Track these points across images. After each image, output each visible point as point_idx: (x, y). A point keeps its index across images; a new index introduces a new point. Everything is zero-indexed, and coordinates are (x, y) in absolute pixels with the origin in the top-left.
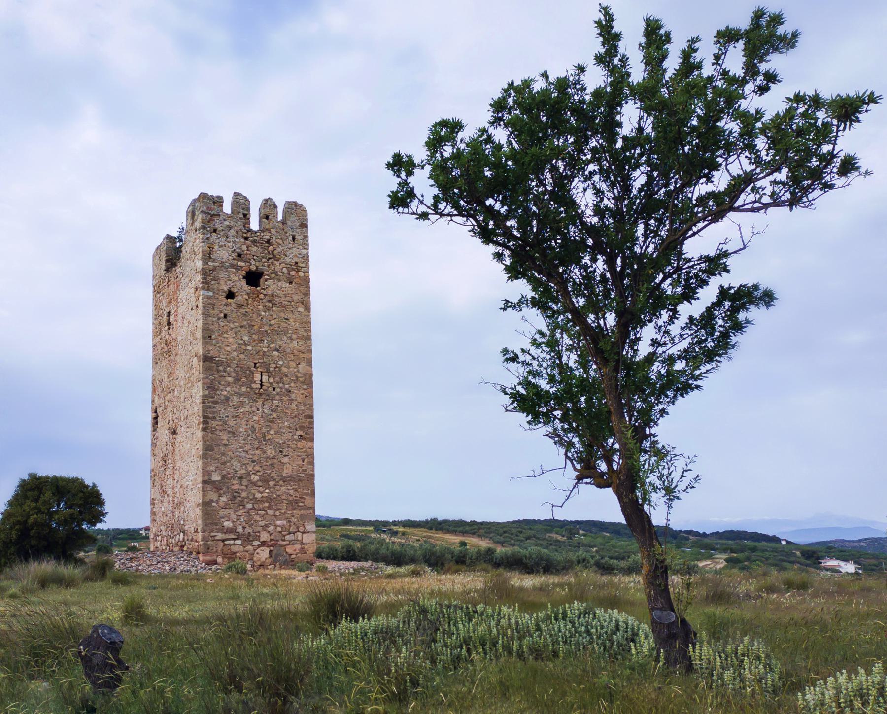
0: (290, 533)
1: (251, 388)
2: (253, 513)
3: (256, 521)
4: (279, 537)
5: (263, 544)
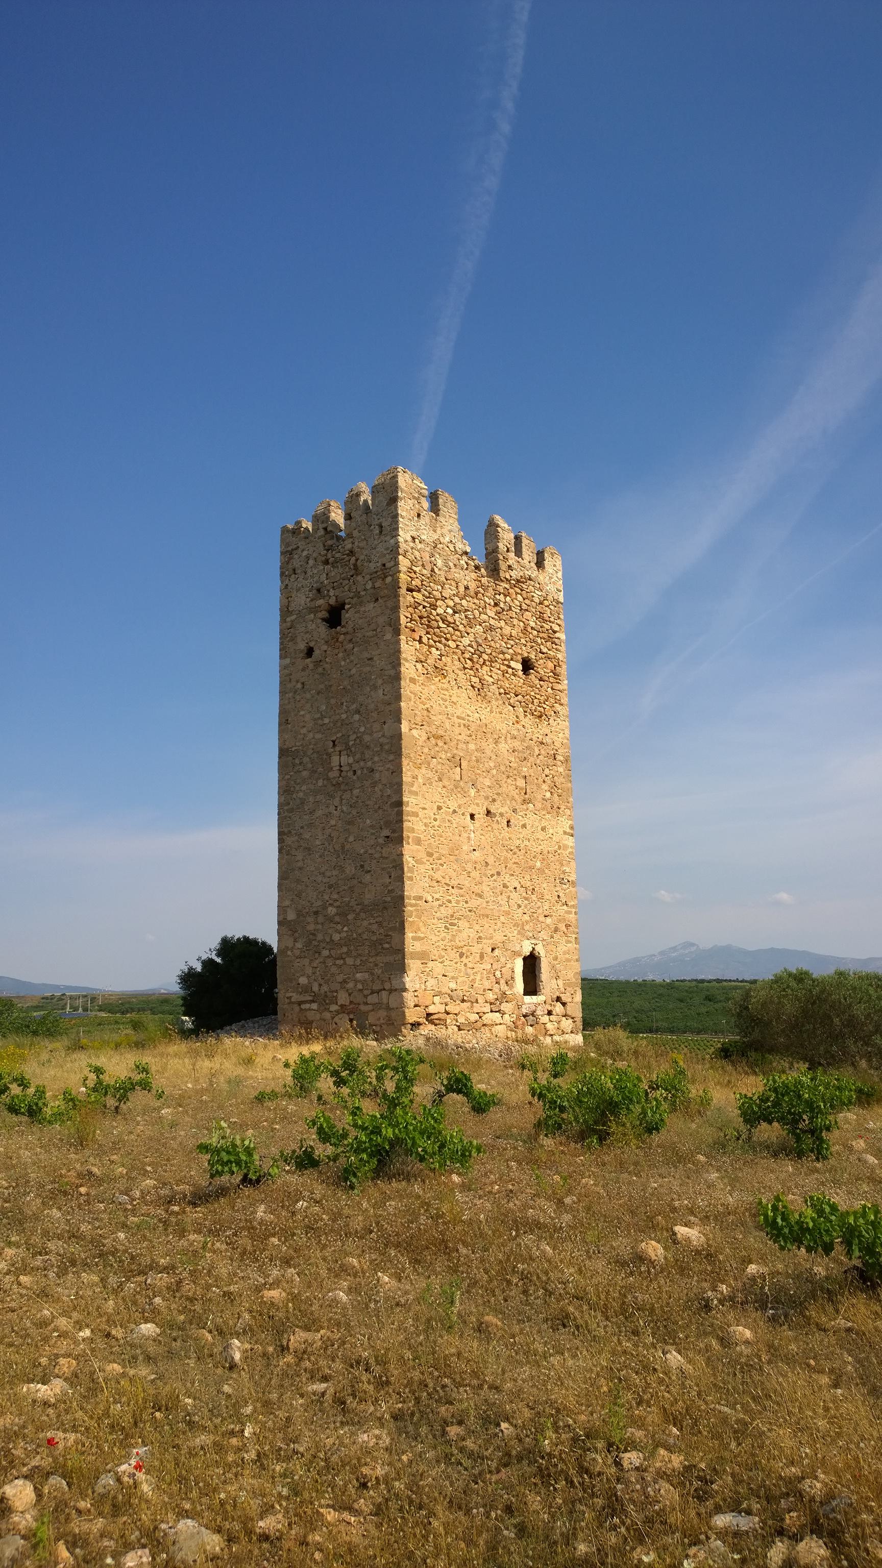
0: (372, 993)
1: (328, 779)
2: (330, 962)
3: (333, 975)
4: (359, 998)
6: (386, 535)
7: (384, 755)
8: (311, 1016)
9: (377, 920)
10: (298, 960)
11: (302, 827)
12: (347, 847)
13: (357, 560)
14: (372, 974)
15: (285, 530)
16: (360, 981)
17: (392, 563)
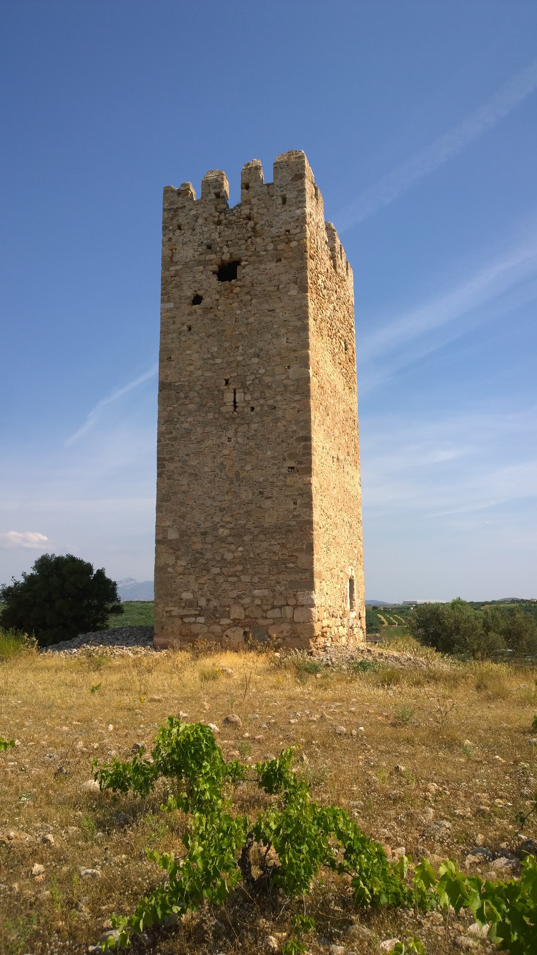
0: (273, 607)
1: (220, 413)
2: (221, 579)
3: (225, 591)
4: (258, 613)
5: (236, 622)
6: (290, 206)
7: (288, 395)
8: (195, 629)
9: (280, 541)
10: (181, 577)
11: (187, 455)
12: (243, 474)
13: (256, 224)
14: (273, 591)
15: (168, 191)
16: (258, 597)
17: (298, 230)
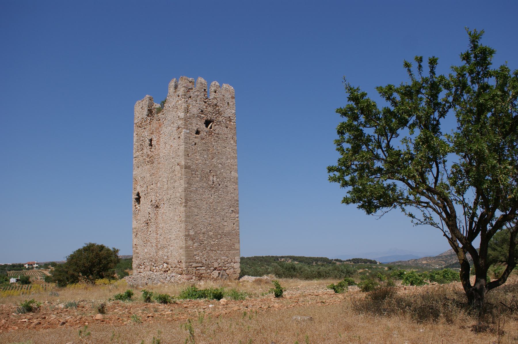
5: (215, 269)
